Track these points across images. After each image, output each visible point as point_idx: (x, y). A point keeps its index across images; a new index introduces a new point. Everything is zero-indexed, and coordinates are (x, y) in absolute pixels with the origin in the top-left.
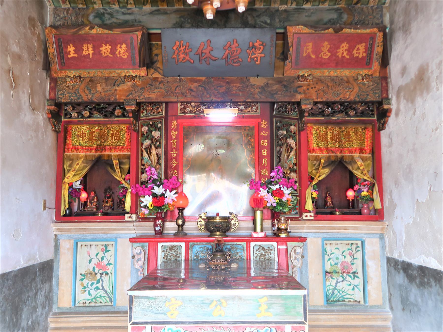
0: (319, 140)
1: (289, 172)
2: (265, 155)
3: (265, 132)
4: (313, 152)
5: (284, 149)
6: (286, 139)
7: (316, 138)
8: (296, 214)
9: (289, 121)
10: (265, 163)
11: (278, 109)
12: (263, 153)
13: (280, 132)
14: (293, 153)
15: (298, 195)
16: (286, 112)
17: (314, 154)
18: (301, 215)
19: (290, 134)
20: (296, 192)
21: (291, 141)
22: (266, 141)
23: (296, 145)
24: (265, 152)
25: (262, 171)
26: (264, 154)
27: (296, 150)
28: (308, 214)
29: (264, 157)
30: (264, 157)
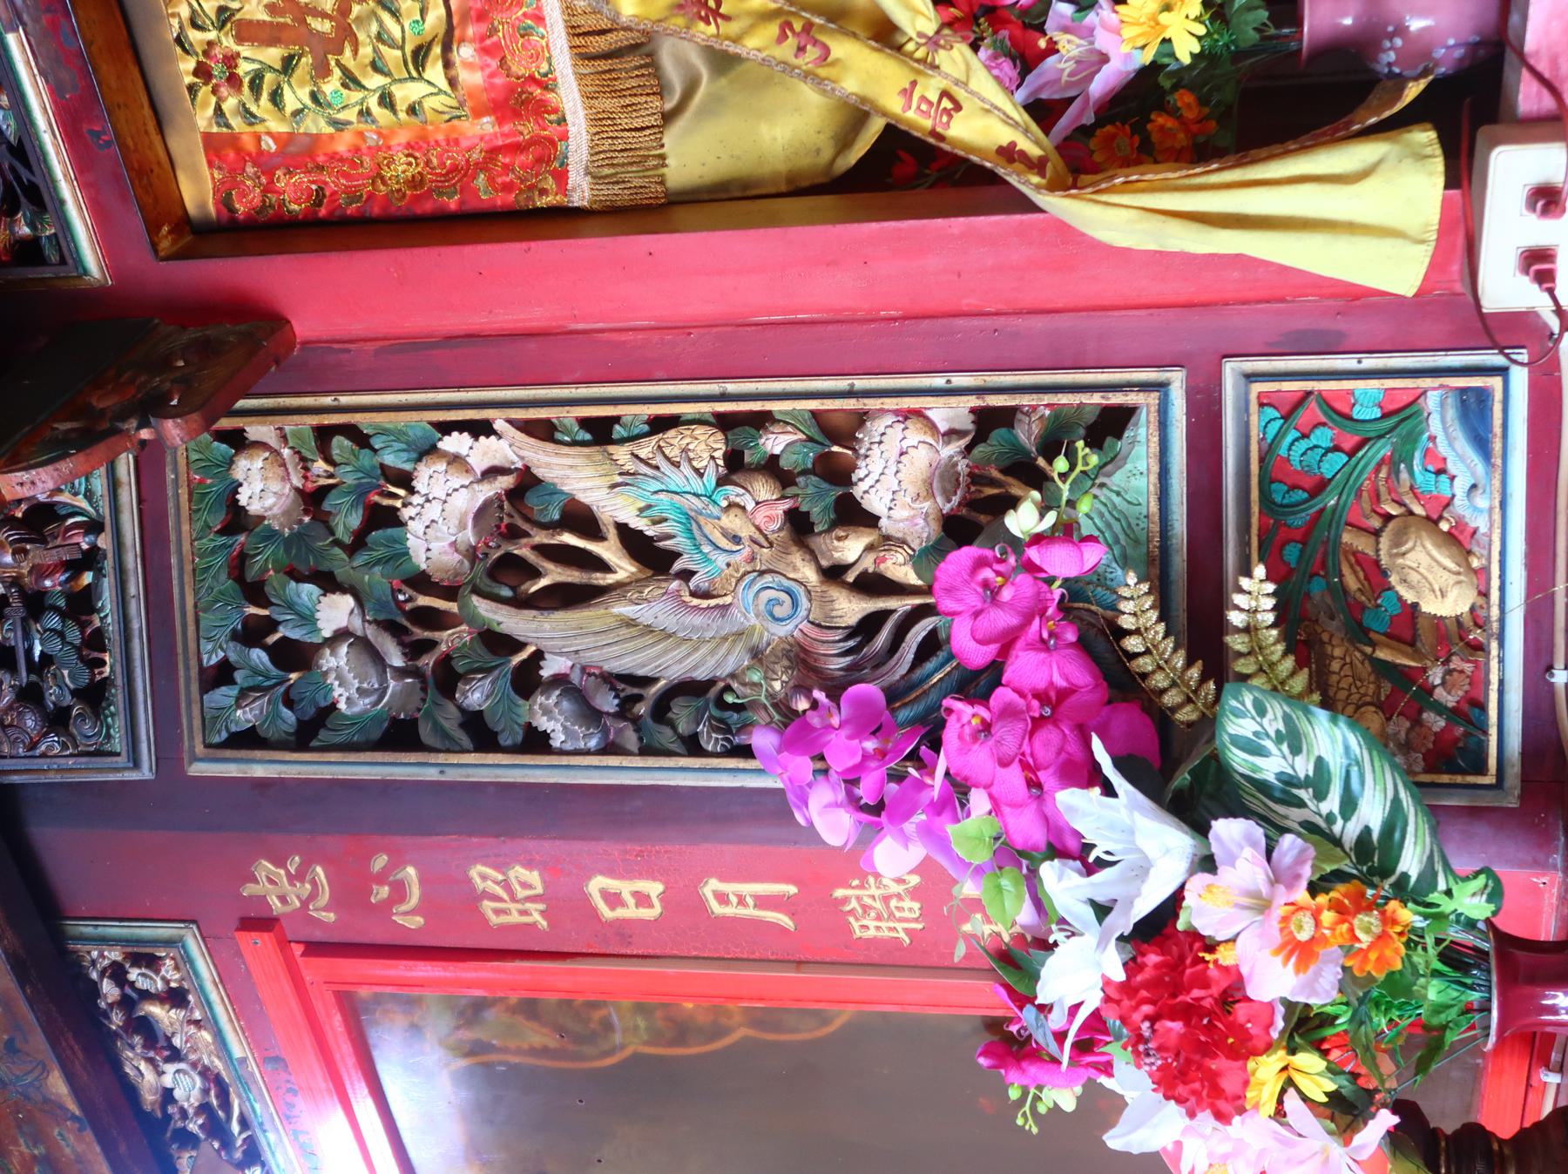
0: (345, 34)
1: (851, 548)
2: (654, 888)
3: (381, 878)
4: (541, 109)
5: (560, 640)
6: (421, 581)
7: (331, 86)
8: (1475, 414)
9: (189, 534)
10: (763, 902)
11: (58, 720)
12: (631, 912)
13: (345, 683)
14: (575, 475)
15: (1177, 380)
16: (81, 604)
17: (569, 96)
18: (1509, 331)
19: (348, 520)
20: (1142, 433)
21: (441, 517)
22: (482, 875)
23: (481, 429)
24: (625, 888)
25: (867, 928)
26: (642, 900)
27: (543, 431)
28: (1507, 227)
29: (684, 903)
30: (684, 903)
